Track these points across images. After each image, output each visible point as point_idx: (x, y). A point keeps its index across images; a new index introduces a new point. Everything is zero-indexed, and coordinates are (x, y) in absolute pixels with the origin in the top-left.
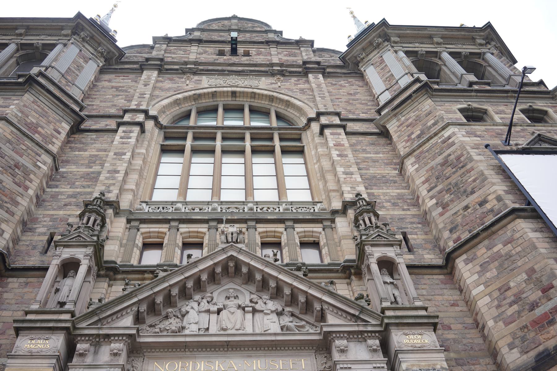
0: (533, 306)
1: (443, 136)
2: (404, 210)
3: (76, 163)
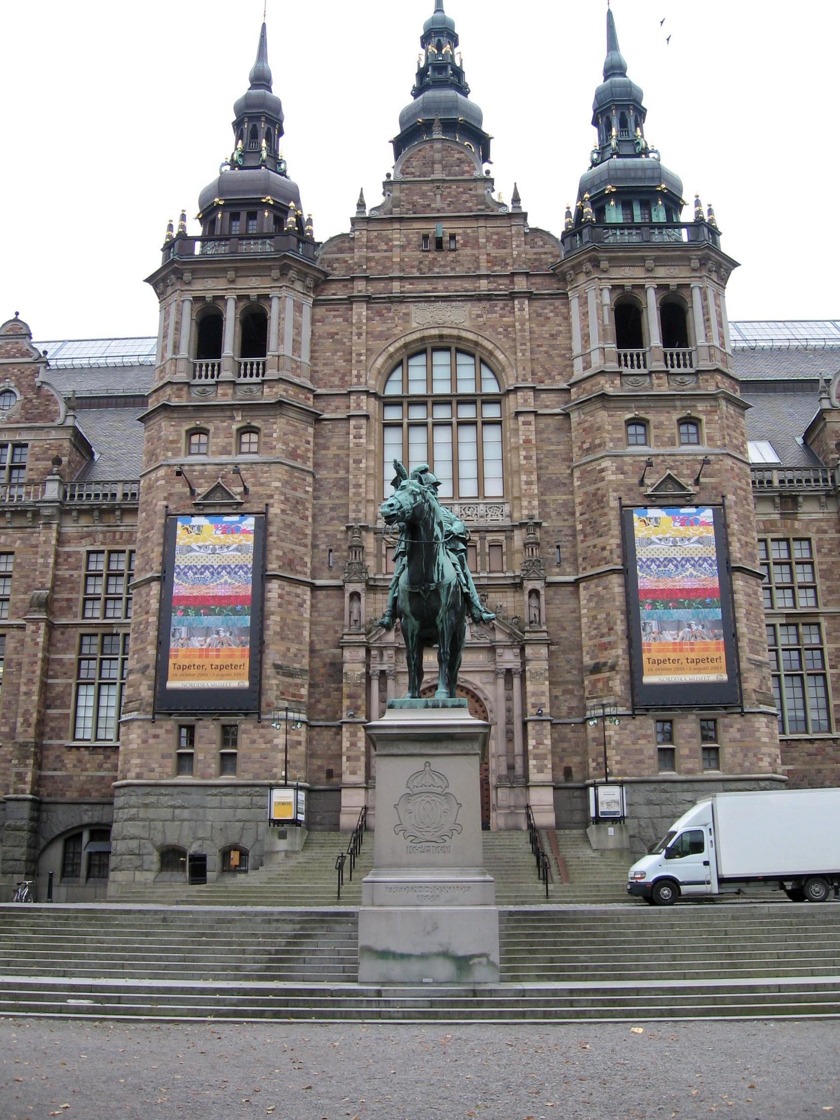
0: (602, 636)
1: (600, 465)
2: (564, 520)
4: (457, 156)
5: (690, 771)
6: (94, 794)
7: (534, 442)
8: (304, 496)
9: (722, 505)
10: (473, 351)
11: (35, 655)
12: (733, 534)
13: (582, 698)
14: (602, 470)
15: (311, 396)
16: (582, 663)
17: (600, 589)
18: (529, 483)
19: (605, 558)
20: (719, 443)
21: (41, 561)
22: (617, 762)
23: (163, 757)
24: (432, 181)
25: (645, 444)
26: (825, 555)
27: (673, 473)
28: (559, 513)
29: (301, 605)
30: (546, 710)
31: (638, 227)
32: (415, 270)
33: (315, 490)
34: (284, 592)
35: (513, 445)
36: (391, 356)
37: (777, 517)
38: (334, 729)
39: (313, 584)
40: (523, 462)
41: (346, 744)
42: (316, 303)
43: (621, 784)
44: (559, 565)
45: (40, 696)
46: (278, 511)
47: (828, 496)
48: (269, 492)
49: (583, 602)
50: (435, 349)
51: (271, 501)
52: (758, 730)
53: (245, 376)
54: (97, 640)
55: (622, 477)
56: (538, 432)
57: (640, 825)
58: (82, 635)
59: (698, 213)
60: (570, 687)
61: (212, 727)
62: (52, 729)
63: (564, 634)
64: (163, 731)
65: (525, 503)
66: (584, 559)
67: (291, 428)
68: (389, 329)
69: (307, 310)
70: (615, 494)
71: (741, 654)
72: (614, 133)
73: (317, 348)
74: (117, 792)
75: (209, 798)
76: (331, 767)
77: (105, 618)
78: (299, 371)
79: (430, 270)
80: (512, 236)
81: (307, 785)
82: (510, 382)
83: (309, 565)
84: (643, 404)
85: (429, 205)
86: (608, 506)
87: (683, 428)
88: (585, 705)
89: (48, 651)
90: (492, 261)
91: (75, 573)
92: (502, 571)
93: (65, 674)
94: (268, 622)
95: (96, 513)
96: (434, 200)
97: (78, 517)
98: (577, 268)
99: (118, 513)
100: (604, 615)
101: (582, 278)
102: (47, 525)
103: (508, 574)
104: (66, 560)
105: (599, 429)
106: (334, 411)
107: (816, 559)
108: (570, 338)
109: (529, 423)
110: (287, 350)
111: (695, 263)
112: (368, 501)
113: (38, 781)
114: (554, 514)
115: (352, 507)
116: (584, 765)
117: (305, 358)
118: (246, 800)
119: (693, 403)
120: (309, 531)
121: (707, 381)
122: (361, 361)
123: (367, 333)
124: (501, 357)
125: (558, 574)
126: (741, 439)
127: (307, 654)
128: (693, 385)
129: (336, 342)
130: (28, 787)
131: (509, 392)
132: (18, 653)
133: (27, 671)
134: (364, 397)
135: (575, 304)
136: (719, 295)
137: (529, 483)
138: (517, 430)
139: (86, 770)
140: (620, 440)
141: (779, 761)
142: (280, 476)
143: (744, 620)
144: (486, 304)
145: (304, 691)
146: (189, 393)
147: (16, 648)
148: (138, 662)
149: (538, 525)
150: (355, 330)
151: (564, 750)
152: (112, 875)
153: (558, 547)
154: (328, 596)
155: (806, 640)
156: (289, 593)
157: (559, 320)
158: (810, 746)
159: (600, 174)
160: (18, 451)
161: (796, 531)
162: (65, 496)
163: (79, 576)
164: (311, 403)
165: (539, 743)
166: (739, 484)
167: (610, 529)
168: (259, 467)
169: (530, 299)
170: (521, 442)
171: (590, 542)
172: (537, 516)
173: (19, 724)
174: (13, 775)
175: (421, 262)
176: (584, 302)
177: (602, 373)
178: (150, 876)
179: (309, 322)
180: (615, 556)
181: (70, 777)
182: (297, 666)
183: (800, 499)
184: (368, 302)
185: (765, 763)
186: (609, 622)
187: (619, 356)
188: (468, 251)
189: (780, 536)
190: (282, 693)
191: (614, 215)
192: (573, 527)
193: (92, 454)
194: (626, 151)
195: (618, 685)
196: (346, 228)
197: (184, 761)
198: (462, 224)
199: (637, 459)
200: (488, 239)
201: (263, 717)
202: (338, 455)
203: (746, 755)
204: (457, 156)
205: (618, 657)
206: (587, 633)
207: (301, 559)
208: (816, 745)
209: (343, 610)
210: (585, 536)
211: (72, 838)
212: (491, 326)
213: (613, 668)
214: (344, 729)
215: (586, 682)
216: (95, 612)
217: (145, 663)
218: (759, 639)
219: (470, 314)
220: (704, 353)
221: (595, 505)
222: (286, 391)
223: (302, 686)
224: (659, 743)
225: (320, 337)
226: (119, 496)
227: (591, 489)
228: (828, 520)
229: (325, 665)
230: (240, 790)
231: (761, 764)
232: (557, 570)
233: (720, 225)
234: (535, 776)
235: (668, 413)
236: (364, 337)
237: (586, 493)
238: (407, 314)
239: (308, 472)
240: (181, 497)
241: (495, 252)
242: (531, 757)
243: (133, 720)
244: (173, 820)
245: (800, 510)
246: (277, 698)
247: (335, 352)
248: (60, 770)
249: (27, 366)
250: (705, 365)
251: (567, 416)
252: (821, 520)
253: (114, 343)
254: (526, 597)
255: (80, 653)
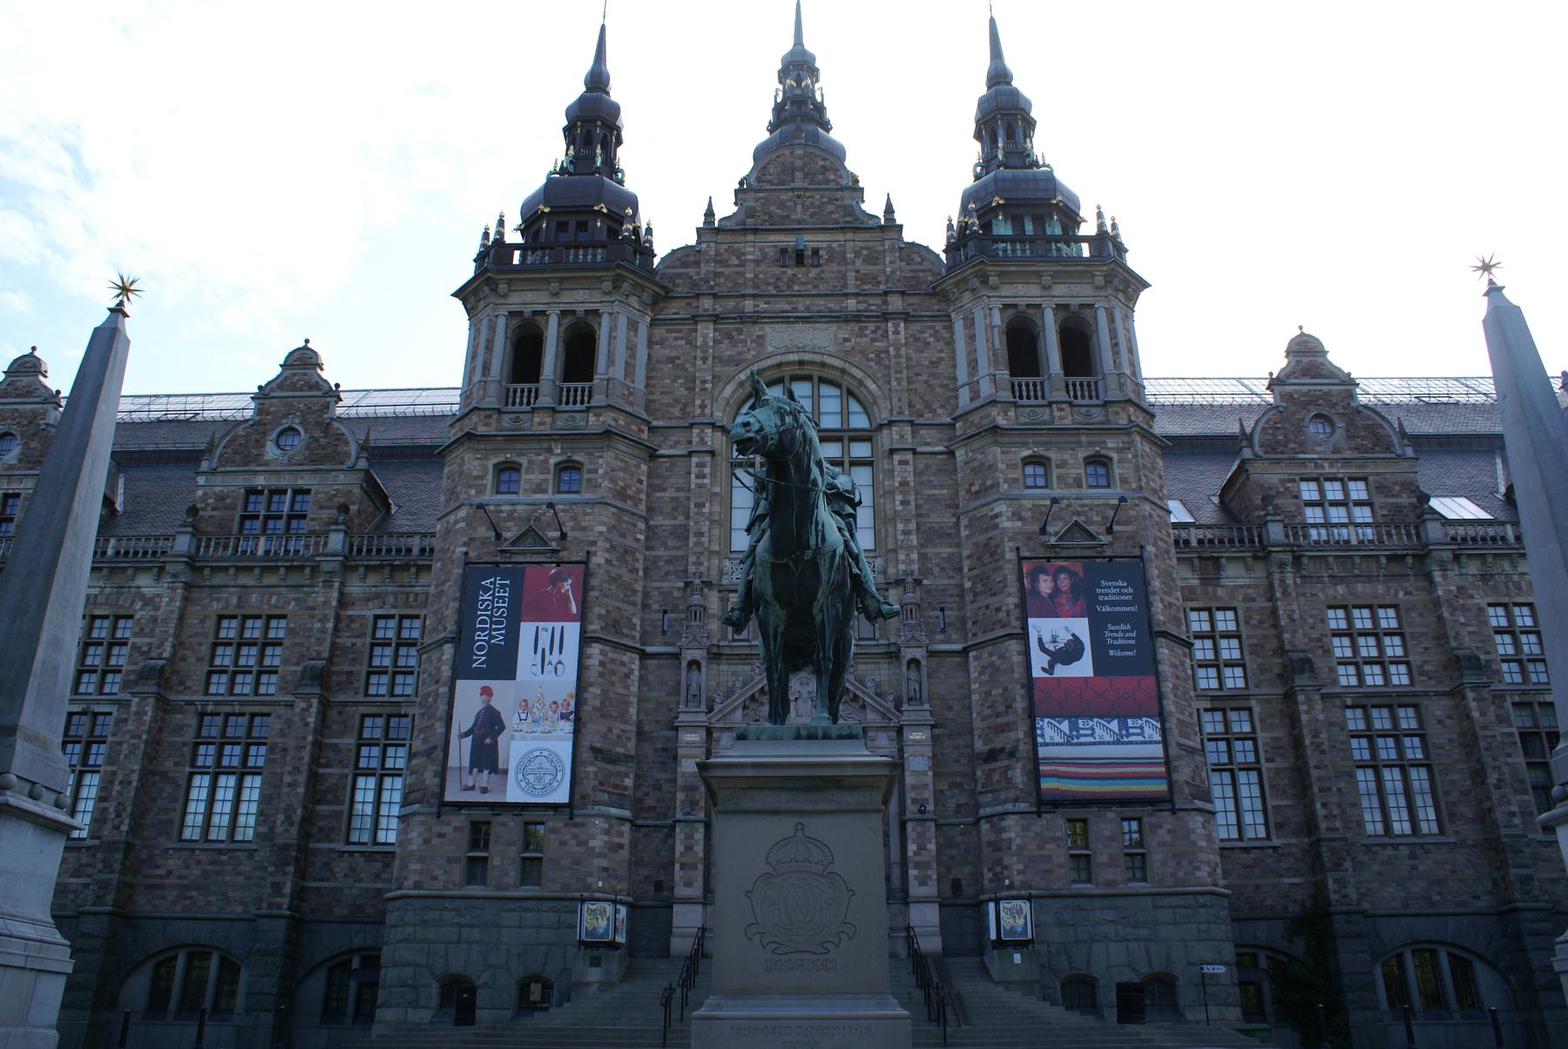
0: (998, 715)
1: (992, 510)
2: (949, 578)
3: (661, 513)
4: (821, 163)
5: (1109, 883)
6: (368, 910)
7: (912, 484)
8: (634, 545)
9: (1141, 557)
10: (839, 380)
11: (305, 738)
12: (1155, 593)
13: (973, 793)
14: (996, 516)
15: (646, 429)
16: (973, 749)
17: (994, 658)
18: (906, 533)
19: (1000, 621)
20: (1134, 485)
21: (318, 625)
22: (1019, 872)
23: (449, 861)
24: (793, 190)
25: (1046, 487)
26: (1254, 627)
27: (1081, 519)
28: (943, 569)
29: (627, 676)
30: (930, 807)
31: (1032, 240)
32: (771, 288)
33: (647, 538)
34: (607, 660)
35: (887, 488)
36: (741, 385)
37: (1196, 582)
38: (666, 830)
39: (643, 651)
40: (900, 508)
41: (679, 848)
42: (654, 323)
43: (1029, 898)
44: (943, 631)
45: (307, 788)
46: (602, 561)
47: (1255, 558)
48: (591, 539)
49: (974, 675)
50: (794, 378)
51: (594, 549)
52: (1193, 830)
53: (567, 403)
54: (380, 721)
55: (1019, 524)
56: (917, 474)
57: (1049, 952)
58: (364, 716)
59: (1101, 226)
60: (958, 779)
61: (512, 824)
62: (321, 830)
63: (950, 715)
64: (451, 829)
65: (902, 557)
66: (974, 623)
67: (621, 464)
68: (739, 353)
69: (643, 330)
70: (1011, 544)
71: (1169, 737)
72: (1000, 145)
73: (654, 374)
74: (390, 905)
75: (505, 915)
76: (661, 878)
77: (392, 695)
78: (631, 399)
79: (789, 287)
80: (885, 251)
81: (630, 899)
82: (883, 416)
83: (638, 628)
84: (1044, 439)
85: (788, 216)
86: (1004, 557)
87: (1091, 469)
88: (977, 802)
89: (322, 734)
90: (862, 279)
91: (359, 642)
92: (874, 639)
93: (340, 762)
94: (586, 695)
95: (387, 569)
96: (795, 211)
97: (365, 574)
98: (962, 284)
99: (413, 570)
100: (1000, 691)
101: (967, 296)
102: (328, 584)
103: (881, 642)
104: (348, 626)
105: (990, 467)
106: (672, 447)
107: (1244, 632)
108: (954, 366)
109: (905, 463)
110: (618, 372)
111: (1099, 280)
112: (712, 553)
113: (299, 894)
114: (936, 570)
115: (692, 559)
116: (977, 877)
117: (640, 383)
118: (553, 917)
119: (1102, 438)
120: (639, 588)
121: (1117, 413)
122: (706, 389)
123: (714, 358)
124: (873, 387)
125: (942, 642)
126: (1159, 482)
127: (633, 736)
128: (1101, 418)
129: (677, 367)
130: (285, 901)
131: (881, 427)
132: (284, 736)
133: (293, 758)
134: (709, 431)
135: (959, 326)
136: (1128, 316)
137: (905, 533)
138: (892, 471)
139: (360, 881)
140: (1015, 480)
141: (1219, 871)
142: (605, 519)
143: (1171, 696)
144: (855, 327)
145: (628, 782)
146: (499, 421)
147: (282, 730)
148: (423, 743)
149: (918, 582)
150: (699, 354)
151: (951, 858)
152: (378, 1012)
153: (942, 610)
154: (660, 667)
155: (1236, 728)
156: (612, 661)
157: (940, 345)
158: (1244, 856)
159: (985, 185)
160: (299, 498)
161: (1219, 599)
162: (351, 550)
163: (364, 644)
164: (645, 436)
165: (922, 848)
166: (1158, 534)
167: (1005, 586)
168: (576, 509)
169: (905, 320)
170: (897, 484)
171: (983, 601)
172: (916, 573)
173: (279, 822)
174: (268, 885)
175: (778, 279)
176: (970, 323)
177: (993, 402)
178: (425, 1015)
179: (645, 342)
180: (1012, 619)
181: (340, 890)
182: (620, 750)
183: (1223, 561)
184: (715, 322)
185: (1203, 873)
186: (1006, 699)
187: (1013, 386)
188: (834, 267)
189: (1200, 604)
190: (601, 784)
191: (1002, 228)
192: (962, 585)
193: (388, 506)
194: (1016, 161)
195: (1018, 775)
196: (692, 240)
197: (476, 869)
198: (827, 237)
199: (1037, 502)
200: (857, 254)
201: (575, 812)
202: (676, 498)
203: (1179, 863)
204: (821, 163)
205: (1018, 740)
206: (979, 713)
207: (630, 620)
208: (1254, 854)
209: (679, 683)
210: (976, 595)
211: (338, 965)
212: (860, 352)
213: (1012, 754)
214: (678, 830)
215: (979, 773)
216: (379, 685)
217: (432, 744)
218: (1188, 720)
219: (836, 336)
220: (1112, 382)
221: (987, 559)
222: (615, 420)
223: (627, 775)
224: (1070, 848)
225: (658, 362)
226: (415, 551)
227: (982, 538)
228: (1256, 587)
229: (656, 750)
230: (545, 905)
231: (1198, 874)
232: (941, 637)
233: (1126, 239)
234: (915, 890)
235: (1073, 449)
236: (710, 362)
237: (976, 545)
238: (761, 337)
239: (640, 516)
240: (484, 541)
241: (865, 269)
242: (911, 865)
243: (413, 814)
244: (459, 942)
245: (1224, 574)
246: (594, 789)
247: (677, 377)
248: (329, 880)
249: (315, 400)
250: (1113, 395)
251: (951, 454)
252: (1249, 586)
253: (425, 393)
254: (904, 669)
255: (360, 737)
